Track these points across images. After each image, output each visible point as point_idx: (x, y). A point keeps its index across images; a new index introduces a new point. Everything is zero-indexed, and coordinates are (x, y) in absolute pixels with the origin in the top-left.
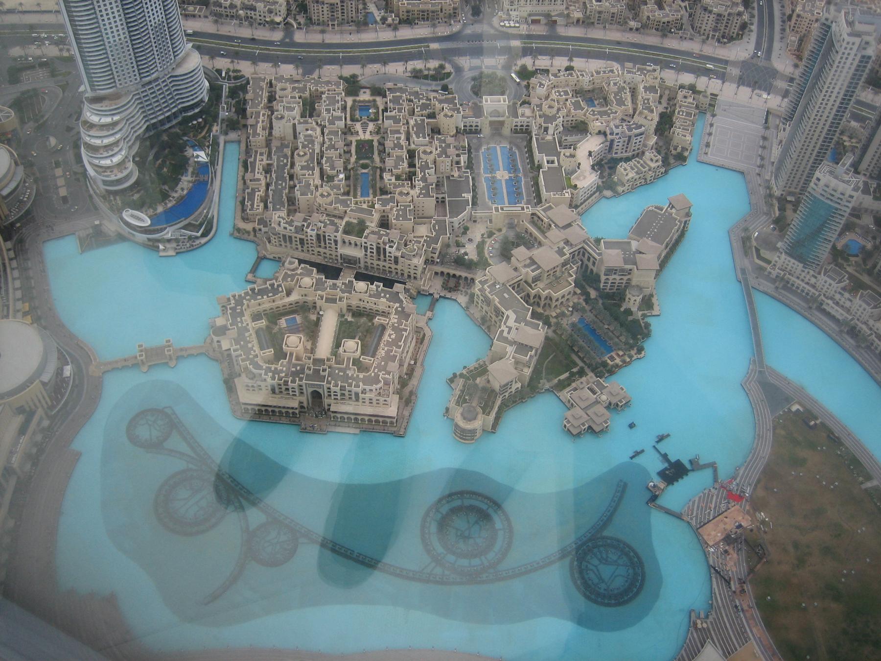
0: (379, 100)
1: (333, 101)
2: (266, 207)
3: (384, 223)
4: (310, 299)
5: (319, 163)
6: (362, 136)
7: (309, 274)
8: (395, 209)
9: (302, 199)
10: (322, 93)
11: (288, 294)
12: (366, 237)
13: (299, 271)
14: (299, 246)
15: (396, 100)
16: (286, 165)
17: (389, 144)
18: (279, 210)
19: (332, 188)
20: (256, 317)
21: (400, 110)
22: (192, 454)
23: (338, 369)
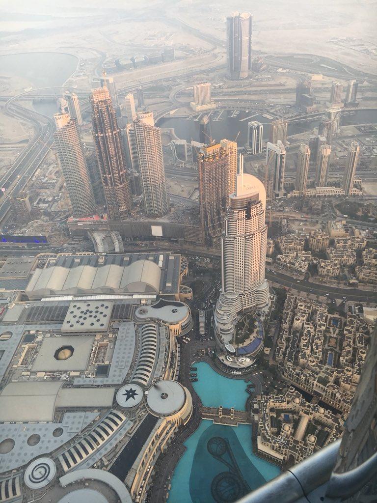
0: (342, 318)
1: (322, 316)
2: (284, 357)
3: (337, 382)
4: (297, 409)
5: (312, 344)
6: (332, 335)
7: (299, 397)
8: (343, 377)
9: (302, 361)
10: (318, 310)
11: (288, 404)
12: (328, 387)
13: (294, 394)
14: (296, 381)
15: (351, 322)
16: (296, 341)
17: (345, 343)
18: (290, 361)
19: (315, 358)
20: (272, 410)
21: (352, 328)
22: (233, 466)
23: (305, 448)
